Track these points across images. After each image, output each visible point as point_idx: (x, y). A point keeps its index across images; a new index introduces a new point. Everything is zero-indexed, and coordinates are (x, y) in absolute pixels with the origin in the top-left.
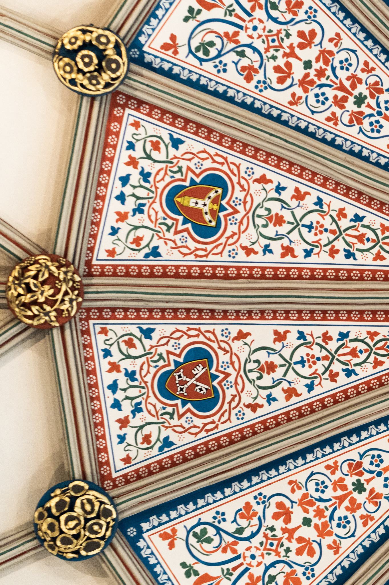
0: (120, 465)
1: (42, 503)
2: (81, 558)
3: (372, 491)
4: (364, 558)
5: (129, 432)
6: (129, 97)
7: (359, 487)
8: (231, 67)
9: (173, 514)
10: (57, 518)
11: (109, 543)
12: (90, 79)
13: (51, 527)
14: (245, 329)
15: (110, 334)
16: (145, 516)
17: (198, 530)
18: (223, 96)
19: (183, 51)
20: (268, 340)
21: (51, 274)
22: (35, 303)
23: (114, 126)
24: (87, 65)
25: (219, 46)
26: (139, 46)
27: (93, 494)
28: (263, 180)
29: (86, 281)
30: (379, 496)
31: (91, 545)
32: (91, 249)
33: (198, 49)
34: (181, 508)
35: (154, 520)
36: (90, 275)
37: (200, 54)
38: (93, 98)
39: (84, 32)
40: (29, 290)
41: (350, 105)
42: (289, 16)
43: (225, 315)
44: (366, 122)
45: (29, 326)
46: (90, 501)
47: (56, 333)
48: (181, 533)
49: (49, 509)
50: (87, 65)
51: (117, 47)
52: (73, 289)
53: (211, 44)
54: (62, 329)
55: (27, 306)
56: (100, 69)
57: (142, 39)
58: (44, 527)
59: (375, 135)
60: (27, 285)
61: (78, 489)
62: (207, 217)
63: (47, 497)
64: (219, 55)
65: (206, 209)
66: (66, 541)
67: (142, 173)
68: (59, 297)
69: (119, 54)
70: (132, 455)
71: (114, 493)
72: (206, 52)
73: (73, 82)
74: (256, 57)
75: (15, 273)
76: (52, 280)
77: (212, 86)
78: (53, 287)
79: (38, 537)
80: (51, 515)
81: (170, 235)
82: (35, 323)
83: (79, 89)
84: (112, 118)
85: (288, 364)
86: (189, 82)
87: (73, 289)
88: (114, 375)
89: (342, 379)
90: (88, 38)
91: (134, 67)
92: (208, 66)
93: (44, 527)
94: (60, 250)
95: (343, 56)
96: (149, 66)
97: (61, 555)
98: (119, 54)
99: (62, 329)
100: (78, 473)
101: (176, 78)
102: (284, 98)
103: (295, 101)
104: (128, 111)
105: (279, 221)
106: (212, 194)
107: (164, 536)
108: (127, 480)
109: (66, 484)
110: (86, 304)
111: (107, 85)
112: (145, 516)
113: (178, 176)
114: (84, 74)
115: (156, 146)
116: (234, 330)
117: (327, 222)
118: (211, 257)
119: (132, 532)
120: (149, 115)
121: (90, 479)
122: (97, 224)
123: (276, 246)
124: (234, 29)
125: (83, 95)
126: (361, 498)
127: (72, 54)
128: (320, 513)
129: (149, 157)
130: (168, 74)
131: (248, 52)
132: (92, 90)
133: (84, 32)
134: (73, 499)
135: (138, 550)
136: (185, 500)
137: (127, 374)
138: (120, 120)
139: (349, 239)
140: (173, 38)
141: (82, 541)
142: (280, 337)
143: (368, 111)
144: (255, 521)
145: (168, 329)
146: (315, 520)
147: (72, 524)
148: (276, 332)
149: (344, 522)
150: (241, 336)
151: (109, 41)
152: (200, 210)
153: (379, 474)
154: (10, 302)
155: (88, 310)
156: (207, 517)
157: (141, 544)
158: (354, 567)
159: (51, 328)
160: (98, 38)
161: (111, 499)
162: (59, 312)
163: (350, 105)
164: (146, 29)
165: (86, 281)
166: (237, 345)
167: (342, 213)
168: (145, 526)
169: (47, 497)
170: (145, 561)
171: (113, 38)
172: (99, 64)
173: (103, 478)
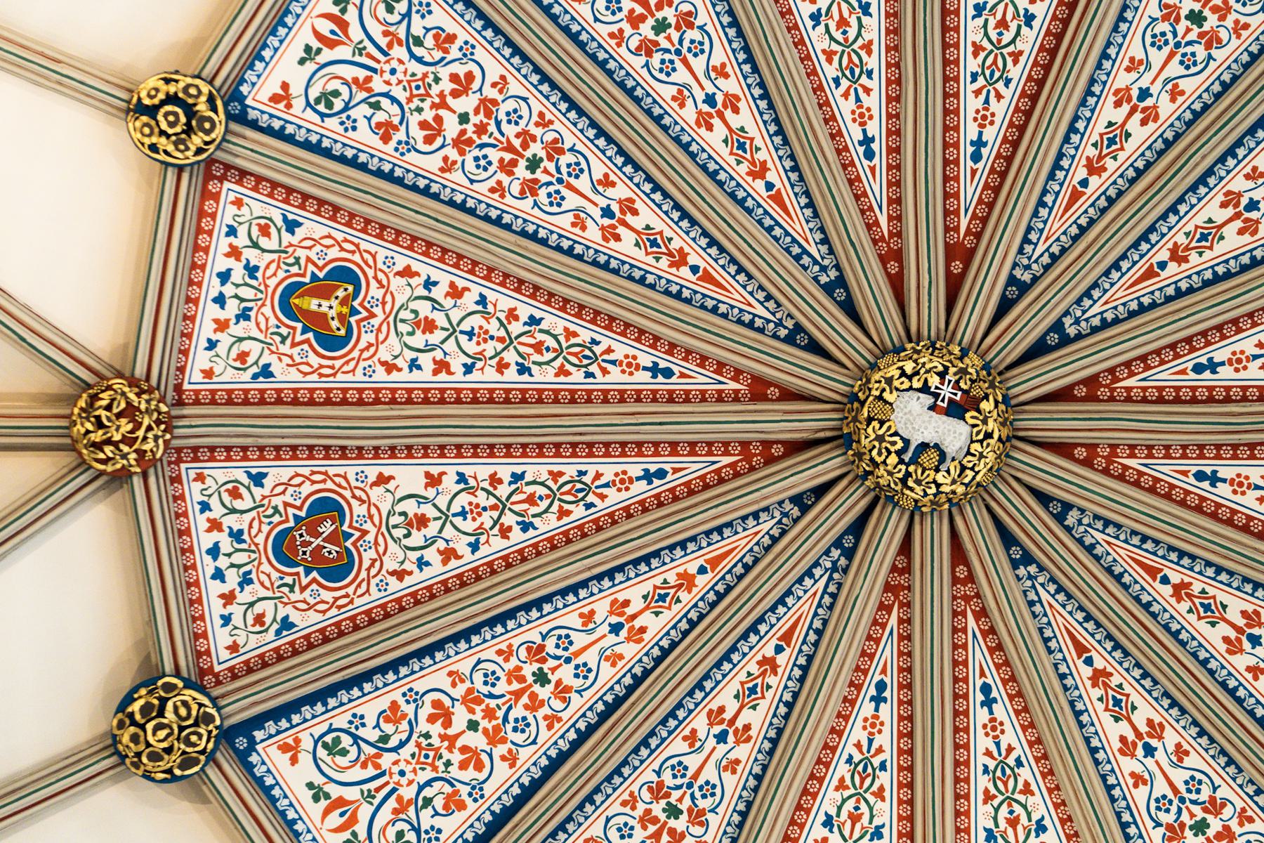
0: (225, 655)
1: (122, 708)
2: (175, 779)
3: (559, 683)
4: (548, 772)
5: (236, 610)
6: (228, 167)
7: (542, 678)
8: (362, 124)
9: (296, 719)
10: (142, 727)
11: (211, 758)
12: (176, 144)
13: (134, 739)
14: (387, 471)
15: (209, 481)
16: (258, 721)
17: (328, 739)
18: (353, 163)
19: (299, 104)
20: (418, 486)
21: (129, 404)
22: (109, 442)
23: (209, 206)
24: (171, 125)
25: (346, 96)
26: (241, 98)
27: (189, 694)
28: (407, 272)
29: (175, 412)
30: (568, 689)
31: (187, 762)
32: (181, 370)
33: (318, 101)
34: (307, 711)
35: (271, 727)
36: (180, 403)
37: (321, 108)
38: (181, 169)
39: (167, 81)
40: (100, 424)
41: (521, 171)
42: (438, 55)
43: (360, 452)
44: (543, 193)
45: (102, 473)
46: (185, 703)
47: (138, 482)
48: (307, 743)
49: (131, 715)
50: (171, 125)
51: (211, 100)
52: (158, 422)
53: (336, 93)
54: (145, 476)
55: (98, 446)
56: (189, 130)
57: (244, 89)
58: (126, 739)
59: (555, 209)
60: (98, 418)
61: (169, 687)
62: (335, 324)
63: (129, 699)
64: (347, 108)
65: (332, 313)
66: (154, 757)
67: (247, 267)
68: (140, 433)
69: (215, 110)
70: (241, 641)
71: (216, 692)
72: (329, 105)
73: (153, 148)
74: (395, 109)
75: (82, 403)
76: (130, 412)
77: (337, 150)
78: (133, 420)
79: (117, 753)
80: (134, 723)
81: (285, 348)
82: (109, 468)
83: (162, 157)
84: (206, 195)
85: (445, 517)
86: (307, 145)
87: (158, 422)
88: (215, 536)
89: (517, 535)
90: (172, 89)
91: (234, 126)
92: (333, 123)
93: (126, 739)
94: (140, 371)
95: (510, 105)
96: (254, 125)
97: (148, 776)
98: (215, 110)
99: (145, 476)
100: (169, 667)
101: (290, 139)
102: (433, 163)
103: (448, 166)
104: (227, 185)
105: (430, 326)
106: (340, 293)
107: (285, 748)
108: (234, 674)
109: (153, 681)
110: (176, 443)
111: (199, 151)
112: (258, 721)
113: (295, 270)
114: (168, 136)
115: (265, 231)
116: (372, 473)
117: (493, 328)
118: (340, 377)
119: (241, 743)
120: (255, 189)
121: (185, 674)
122: (189, 336)
123: (426, 360)
124: (365, 73)
125: (167, 164)
126: (544, 692)
127: (152, 111)
128: (490, 714)
129: (255, 245)
130: (280, 135)
131: (385, 103)
132: (180, 158)
133: (167, 81)
134: (163, 701)
135: (249, 767)
136: (311, 699)
137: (231, 534)
138: (216, 197)
139: (522, 349)
140: (285, 86)
141: (176, 757)
142: (433, 481)
143: (544, 178)
144: (404, 725)
145: (285, 474)
146: (484, 723)
147: (162, 734)
148: (428, 475)
149: (522, 725)
150: (382, 480)
151: (200, 92)
152: (325, 315)
153: (568, 660)
154: (75, 441)
155: (179, 450)
156: (341, 721)
157: (254, 758)
158: (536, 785)
159: (131, 475)
160: (186, 89)
161: (214, 700)
162: (141, 453)
163: (521, 171)
164: (250, 76)
165: (175, 412)
166: (376, 493)
167: (512, 315)
168: (259, 735)
169: (129, 699)
170: (260, 781)
171: (205, 89)
172: (188, 124)
173: (202, 673)
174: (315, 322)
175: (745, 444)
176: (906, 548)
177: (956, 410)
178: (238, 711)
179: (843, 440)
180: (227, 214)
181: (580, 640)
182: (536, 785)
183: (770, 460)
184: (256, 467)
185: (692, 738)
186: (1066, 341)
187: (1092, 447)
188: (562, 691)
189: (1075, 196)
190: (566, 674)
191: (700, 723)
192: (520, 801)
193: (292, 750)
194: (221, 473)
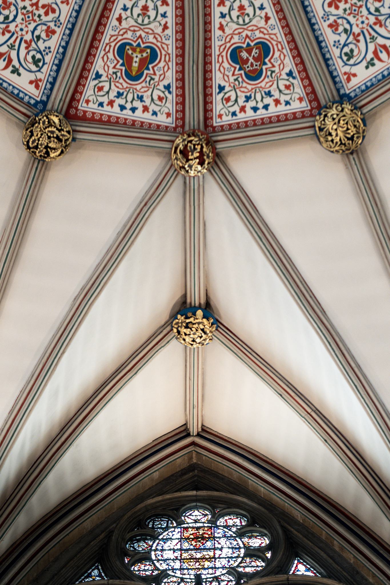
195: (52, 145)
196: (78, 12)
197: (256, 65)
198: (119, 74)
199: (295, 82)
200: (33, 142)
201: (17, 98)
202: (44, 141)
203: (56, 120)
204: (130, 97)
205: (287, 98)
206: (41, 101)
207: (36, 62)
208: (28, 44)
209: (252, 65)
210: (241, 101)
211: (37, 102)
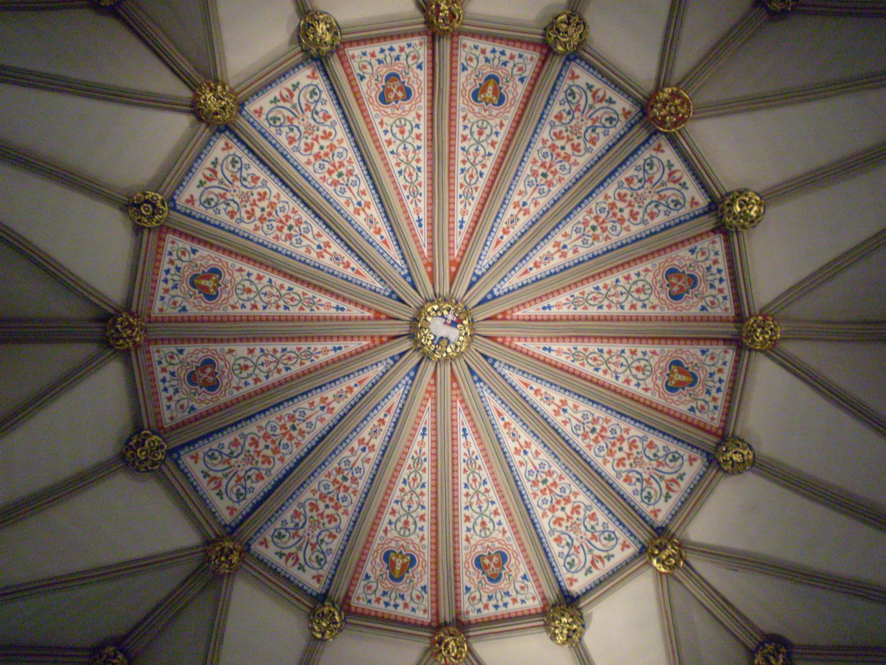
16: (182, 447)
41: (286, 230)
63: (130, 439)
112: (182, 447)
116: (227, 348)
126: (294, 433)
135: (178, 465)
142: (251, 351)
163: (286, 230)
166: (228, 357)
174: (204, 289)
175: (372, 337)
176: (434, 376)
177: (454, 324)
178: (175, 443)
179: (411, 336)
180: (168, 246)
181: (308, 413)
182: (292, 470)
183: (382, 343)
184: (180, 346)
185: (352, 450)
186: (494, 297)
187: (504, 338)
188: (302, 433)
189: (498, 242)
190: (303, 426)
191: (355, 444)
192: (286, 476)
193: (195, 458)
194: (167, 349)
195: (564, 26)
196: (535, 132)
197: (390, 86)
198: (504, 80)
199: (358, 71)
200: (579, 29)
201: (591, 65)
202: (571, 30)
203: (560, 48)
204: (496, 62)
205: (364, 58)
206: (570, 60)
207: (573, 94)
208: (577, 108)
209: (394, 86)
210: (403, 56)
211: (574, 60)
